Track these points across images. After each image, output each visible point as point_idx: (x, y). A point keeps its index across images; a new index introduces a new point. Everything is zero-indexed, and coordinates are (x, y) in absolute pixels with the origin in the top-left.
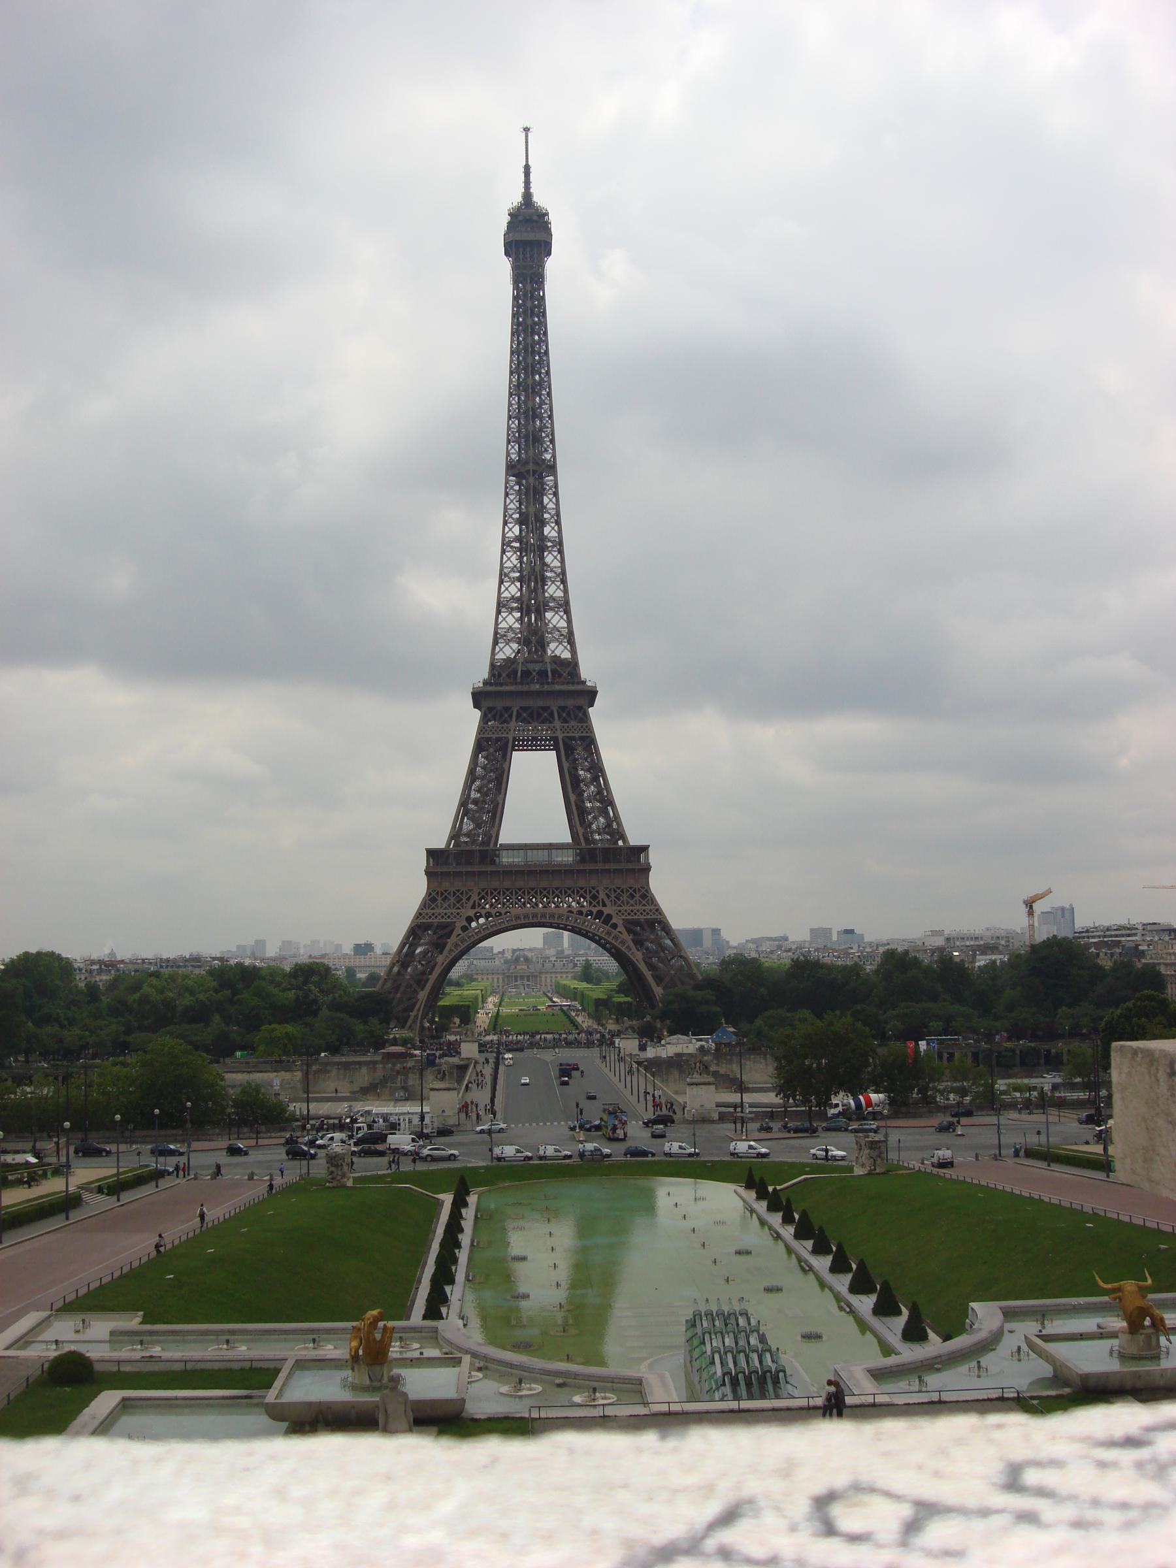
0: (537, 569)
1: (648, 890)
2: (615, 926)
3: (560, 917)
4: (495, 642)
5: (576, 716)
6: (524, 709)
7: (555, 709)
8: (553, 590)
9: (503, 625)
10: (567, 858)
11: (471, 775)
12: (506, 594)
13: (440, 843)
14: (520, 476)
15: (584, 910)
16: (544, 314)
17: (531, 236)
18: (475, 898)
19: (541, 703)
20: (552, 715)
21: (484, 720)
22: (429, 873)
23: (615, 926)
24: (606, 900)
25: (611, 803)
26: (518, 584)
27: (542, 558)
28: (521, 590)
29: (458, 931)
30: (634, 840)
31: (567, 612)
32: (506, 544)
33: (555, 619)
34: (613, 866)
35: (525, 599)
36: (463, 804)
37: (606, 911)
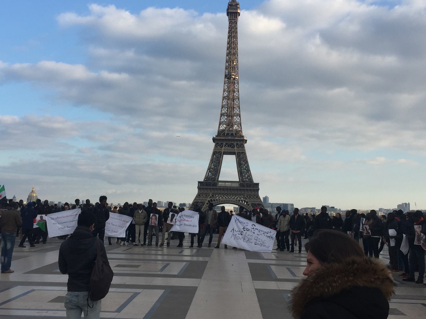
0: (232, 105)
1: (258, 195)
2: (248, 205)
3: (234, 201)
4: (220, 125)
5: (241, 146)
6: (227, 144)
7: (235, 144)
8: (236, 111)
9: (222, 120)
10: (237, 185)
11: (212, 161)
12: (223, 112)
13: (202, 180)
14: (228, 78)
15: (240, 200)
16: (237, 32)
17: (234, 11)
18: (211, 195)
19: (230, 143)
20: (234, 146)
21: (216, 146)
22: (198, 188)
23: (248, 205)
24: (247, 198)
25: (250, 171)
26: (227, 109)
27: (233, 101)
28: (227, 110)
29: (206, 204)
30: (255, 181)
31: (240, 117)
32: (224, 98)
33: (236, 119)
34: (248, 188)
35: (228, 113)
36: (209, 169)
37: (246, 201)
